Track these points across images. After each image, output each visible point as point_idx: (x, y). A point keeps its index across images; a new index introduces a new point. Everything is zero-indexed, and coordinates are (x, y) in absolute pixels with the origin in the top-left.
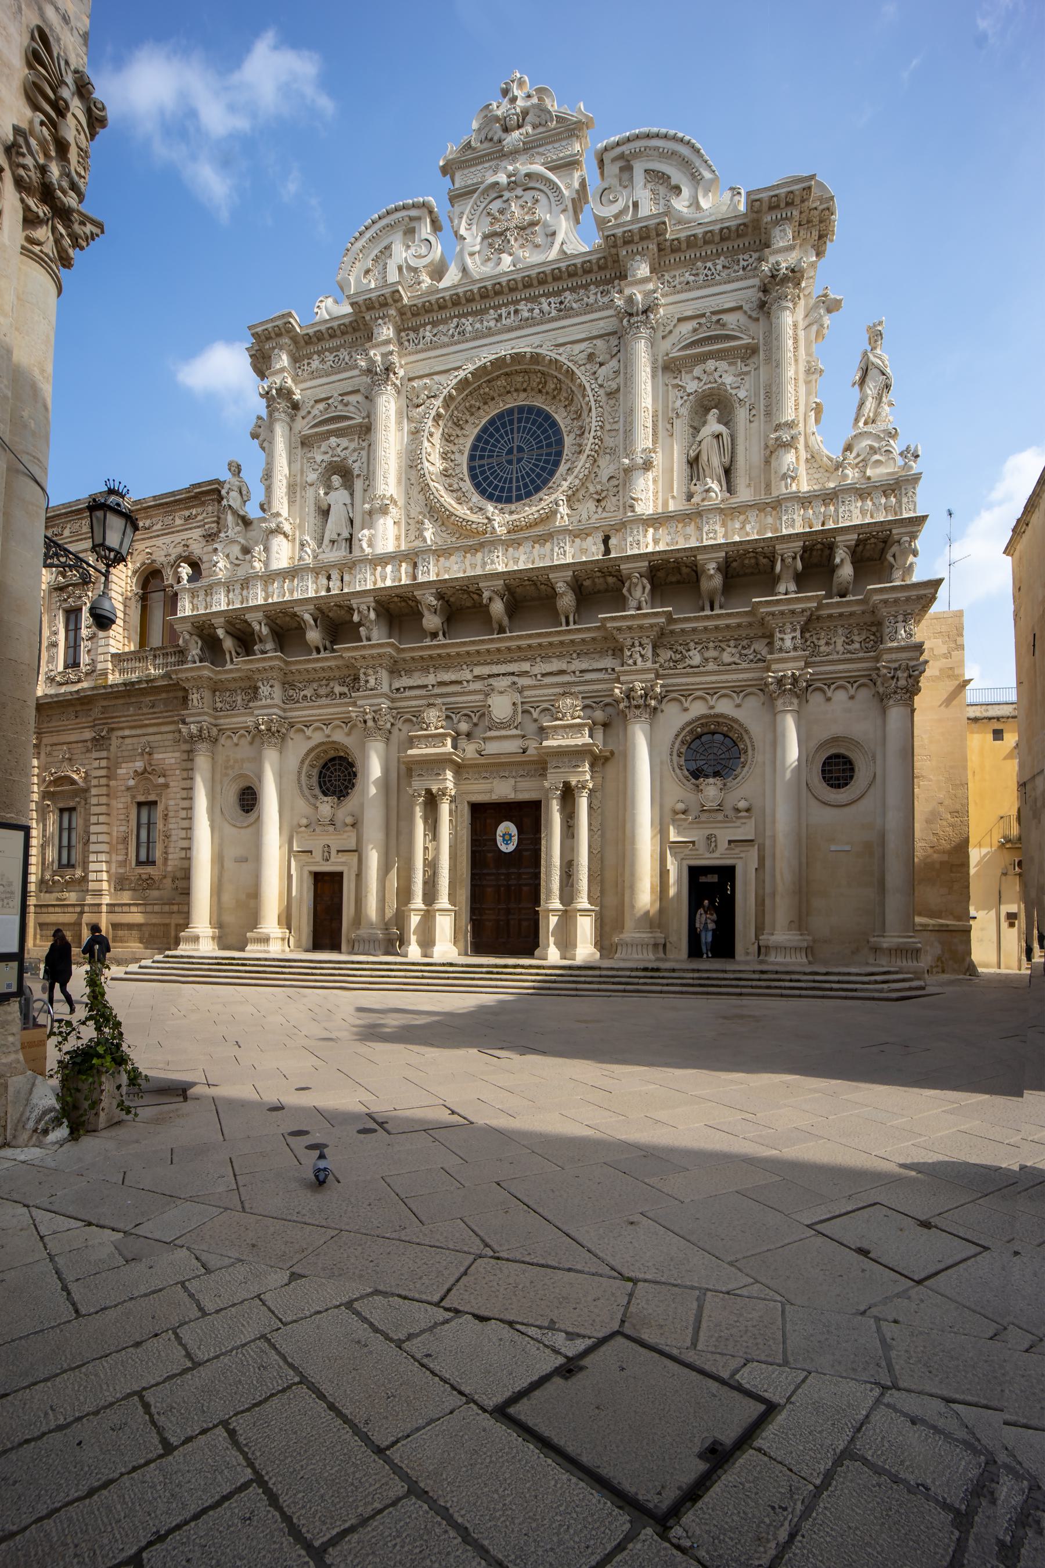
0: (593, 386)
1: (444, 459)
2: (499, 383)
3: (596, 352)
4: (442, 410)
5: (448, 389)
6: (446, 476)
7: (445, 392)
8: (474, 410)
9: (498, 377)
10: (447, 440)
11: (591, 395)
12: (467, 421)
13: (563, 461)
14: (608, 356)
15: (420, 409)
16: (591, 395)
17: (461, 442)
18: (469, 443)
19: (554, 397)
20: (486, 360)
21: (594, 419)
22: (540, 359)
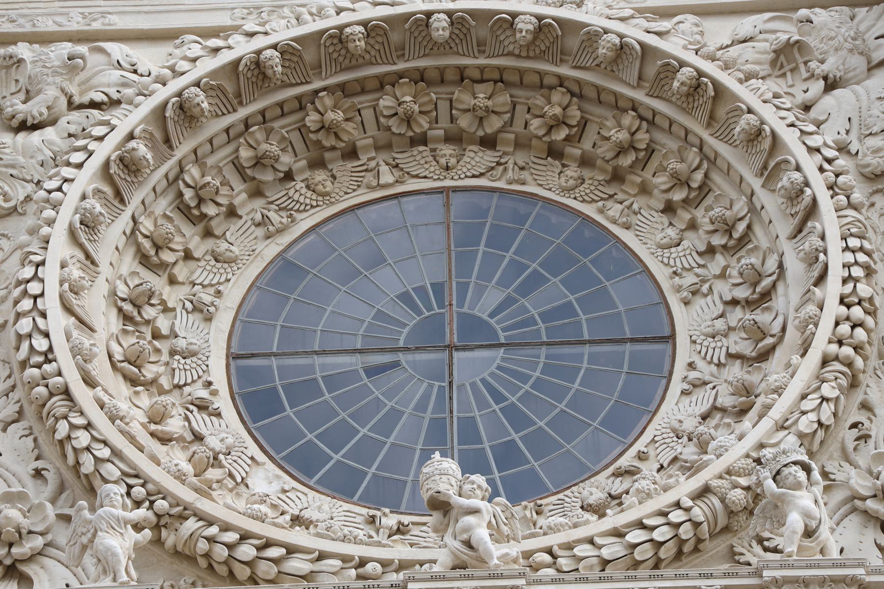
0: (815, 141)
1: (127, 318)
2: (386, 102)
3: (812, 41)
4: (142, 149)
5: (175, 85)
6: (133, 381)
7: (162, 93)
8: (268, 176)
9: (382, 83)
10: (144, 260)
11: (810, 164)
12: (232, 213)
13: (676, 386)
14: (858, 63)
15: (36, 137)
16: (810, 164)
17: (200, 276)
18: (234, 293)
19: (617, 177)
20: (345, 18)
21: (834, 245)
22: (573, 43)
